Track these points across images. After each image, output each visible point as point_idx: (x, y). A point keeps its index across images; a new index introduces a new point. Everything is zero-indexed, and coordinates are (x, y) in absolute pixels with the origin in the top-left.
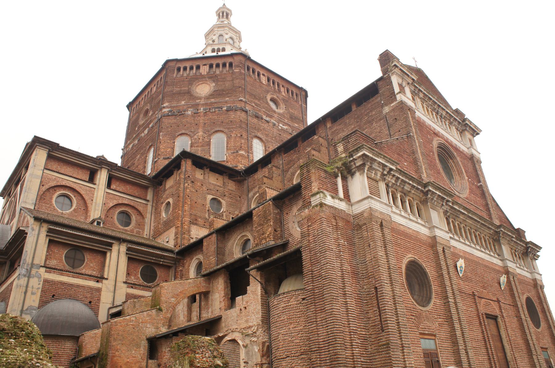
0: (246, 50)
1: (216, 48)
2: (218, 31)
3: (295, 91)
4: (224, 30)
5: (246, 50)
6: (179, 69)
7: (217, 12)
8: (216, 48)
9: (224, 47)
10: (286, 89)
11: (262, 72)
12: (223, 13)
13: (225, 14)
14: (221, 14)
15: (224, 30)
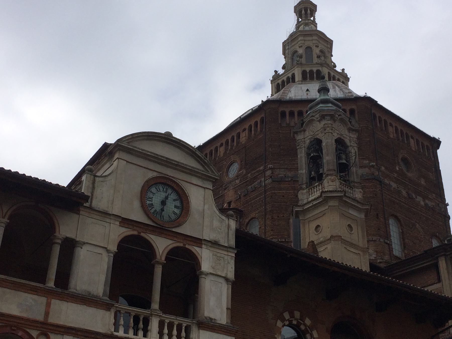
0: (343, 70)
1: (308, 70)
2: (305, 41)
3: (426, 143)
4: (312, 40)
5: (343, 70)
6: (283, 114)
7: (295, 7)
8: (308, 70)
9: (320, 69)
10: (415, 140)
11: (389, 121)
12: (306, 10)
13: (309, 11)
14: (303, 12)
15: (312, 40)
